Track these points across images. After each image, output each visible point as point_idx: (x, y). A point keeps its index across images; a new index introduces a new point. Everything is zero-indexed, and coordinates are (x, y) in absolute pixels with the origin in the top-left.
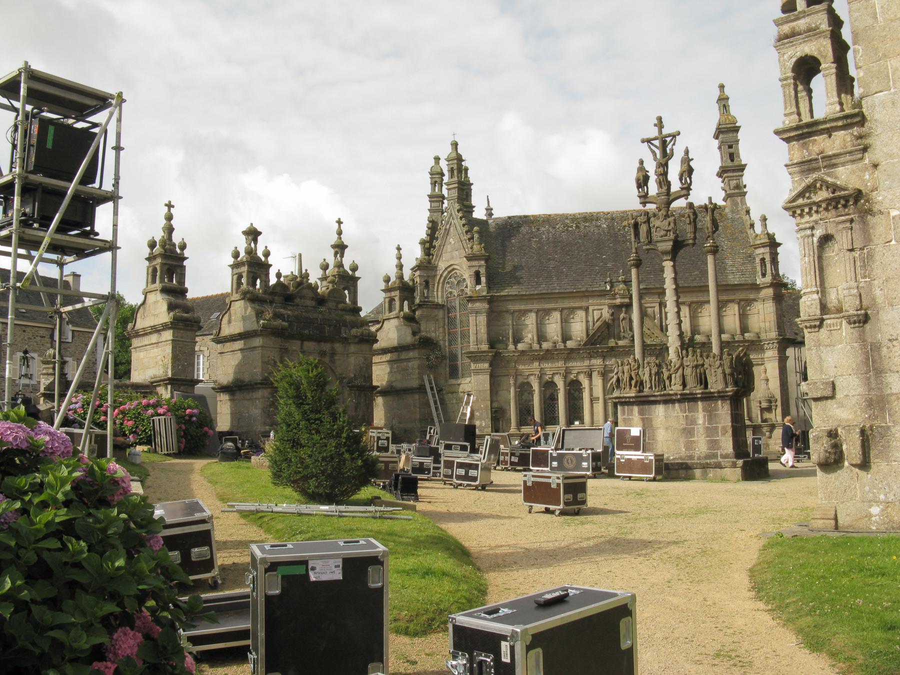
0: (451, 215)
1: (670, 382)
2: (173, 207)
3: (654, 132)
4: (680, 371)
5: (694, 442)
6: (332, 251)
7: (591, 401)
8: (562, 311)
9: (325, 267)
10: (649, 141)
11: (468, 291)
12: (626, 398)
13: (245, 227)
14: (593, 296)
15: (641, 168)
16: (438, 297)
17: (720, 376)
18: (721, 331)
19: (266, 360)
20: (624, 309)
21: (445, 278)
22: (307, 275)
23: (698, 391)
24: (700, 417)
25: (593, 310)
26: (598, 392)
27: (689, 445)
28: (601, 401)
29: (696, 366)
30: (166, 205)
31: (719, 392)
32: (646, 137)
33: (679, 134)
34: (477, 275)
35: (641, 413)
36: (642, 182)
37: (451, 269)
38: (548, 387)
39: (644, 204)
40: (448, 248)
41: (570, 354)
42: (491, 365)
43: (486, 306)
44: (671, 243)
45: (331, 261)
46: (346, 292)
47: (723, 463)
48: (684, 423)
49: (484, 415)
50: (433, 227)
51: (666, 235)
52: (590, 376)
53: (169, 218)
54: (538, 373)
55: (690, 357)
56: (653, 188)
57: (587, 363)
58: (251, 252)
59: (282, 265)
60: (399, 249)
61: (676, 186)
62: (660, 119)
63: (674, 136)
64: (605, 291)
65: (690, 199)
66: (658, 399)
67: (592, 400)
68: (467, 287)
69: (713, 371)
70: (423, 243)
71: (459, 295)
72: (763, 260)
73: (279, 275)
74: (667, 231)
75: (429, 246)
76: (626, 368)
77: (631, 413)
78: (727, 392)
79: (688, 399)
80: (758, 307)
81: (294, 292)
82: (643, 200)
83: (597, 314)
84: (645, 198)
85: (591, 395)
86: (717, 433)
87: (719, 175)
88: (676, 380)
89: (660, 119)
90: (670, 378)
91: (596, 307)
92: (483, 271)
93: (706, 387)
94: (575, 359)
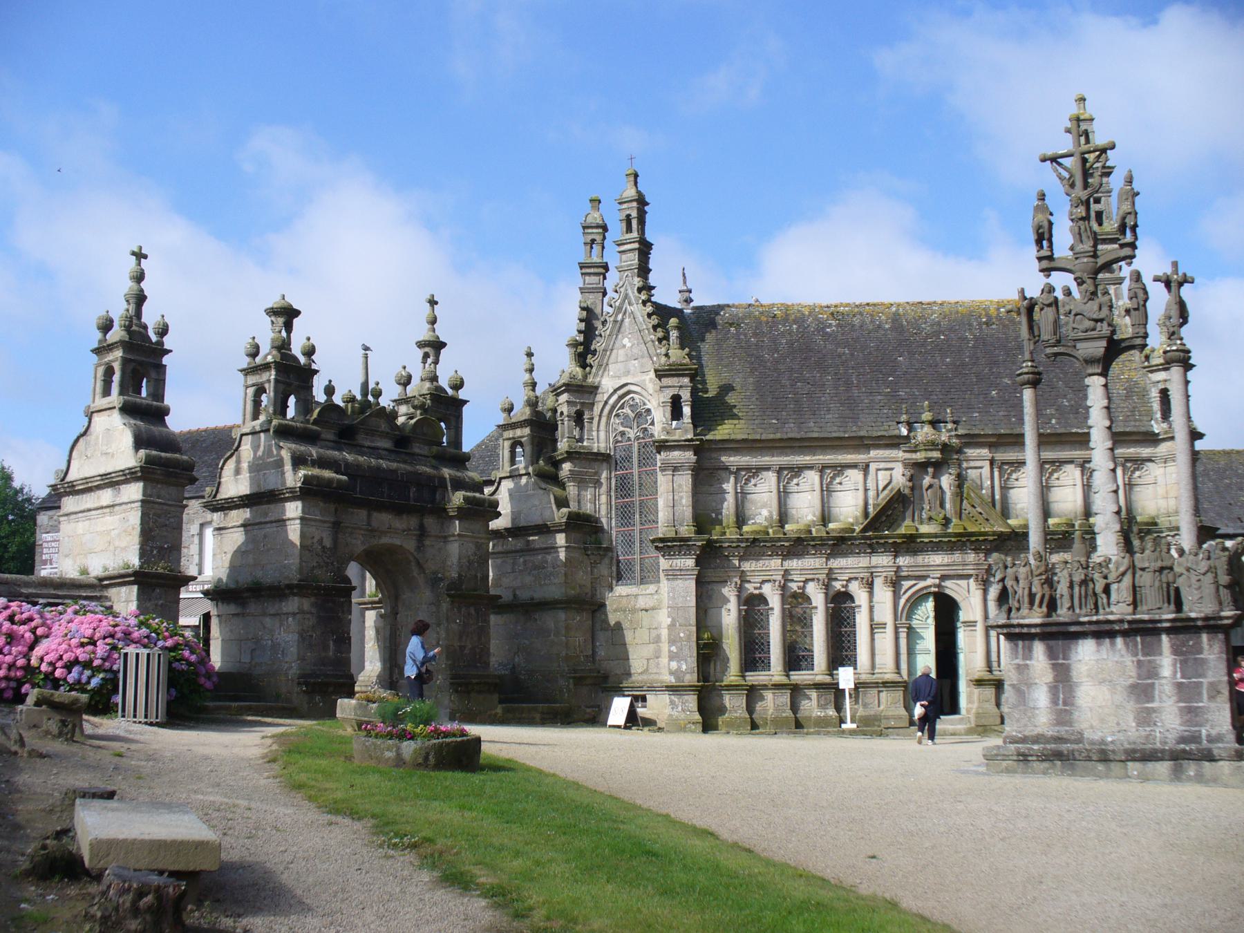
0: (626, 296)
1: (1109, 598)
2: (145, 257)
3: (1065, 143)
4: (1127, 580)
5: (1154, 710)
6: (420, 353)
7: (872, 629)
8: (822, 469)
9: (406, 381)
10: (1054, 159)
11: (658, 432)
12: (1022, 626)
13: (273, 301)
14: (878, 447)
16: (599, 439)
17: (1209, 589)
18: (1046, 513)
19: (309, 542)
20: (930, 470)
21: (613, 407)
22: (378, 394)
23: (1165, 617)
24: (1166, 663)
26: (885, 613)
27: (1146, 717)
28: (890, 629)
29: (1162, 569)
30: (134, 253)
31: (1206, 619)
32: (1050, 152)
34: (676, 403)
35: (1051, 654)
37: (623, 392)
38: (795, 603)
39: (1047, 271)
40: (618, 354)
41: (840, 544)
42: (698, 563)
43: (689, 456)
44: (1104, 343)
45: (417, 371)
46: (443, 424)
47: (1216, 752)
48: (1134, 674)
49: (686, 651)
50: (589, 319)
51: (1094, 329)
52: (870, 585)
53: (139, 277)
54: (779, 578)
55: (1147, 552)
58: (283, 346)
59: (338, 377)
64: (900, 437)
66: (1086, 628)
67: (874, 627)
68: (652, 423)
69: (1194, 579)
70: (574, 344)
71: (638, 438)
72: (1164, 394)
73: (330, 390)
74: (1096, 321)
75: (585, 349)
76: (1022, 571)
77: (1028, 654)
78: (1221, 618)
79: (1141, 631)
80: (1154, 471)
81: (353, 423)
82: (1045, 264)
83: (883, 478)
84: (1049, 264)
85: (872, 619)
86: (1200, 694)
88: (1121, 592)
90: (1107, 590)
91: (882, 465)
92: (686, 395)
93: (1179, 606)
94: (844, 554)
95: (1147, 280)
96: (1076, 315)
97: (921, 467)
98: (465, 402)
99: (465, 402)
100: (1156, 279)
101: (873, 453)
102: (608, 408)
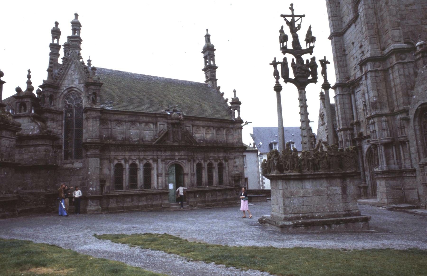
10: (284, 16)
20: (176, 126)
25: (160, 124)
32: (284, 14)
33: (304, 16)
36: (283, 38)
39: (284, 53)
51: (304, 73)
52: (157, 161)
56: (289, 45)
57: (155, 154)
60: (29, 71)
61: (304, 45)
62: (292, 5)
63: (301, 16)
65: (314, 55)
67: (158, 175)
68: (82, 102)
84: (285, 50)
87: (204, 70)
89: (292, 5)
91: (161, 123)
96: (298, 68)
97: (173, 124)
98: (4, 82)
99: (4, 82)
100: (320, 61)
101: (159, 119)
102: (62, 96)
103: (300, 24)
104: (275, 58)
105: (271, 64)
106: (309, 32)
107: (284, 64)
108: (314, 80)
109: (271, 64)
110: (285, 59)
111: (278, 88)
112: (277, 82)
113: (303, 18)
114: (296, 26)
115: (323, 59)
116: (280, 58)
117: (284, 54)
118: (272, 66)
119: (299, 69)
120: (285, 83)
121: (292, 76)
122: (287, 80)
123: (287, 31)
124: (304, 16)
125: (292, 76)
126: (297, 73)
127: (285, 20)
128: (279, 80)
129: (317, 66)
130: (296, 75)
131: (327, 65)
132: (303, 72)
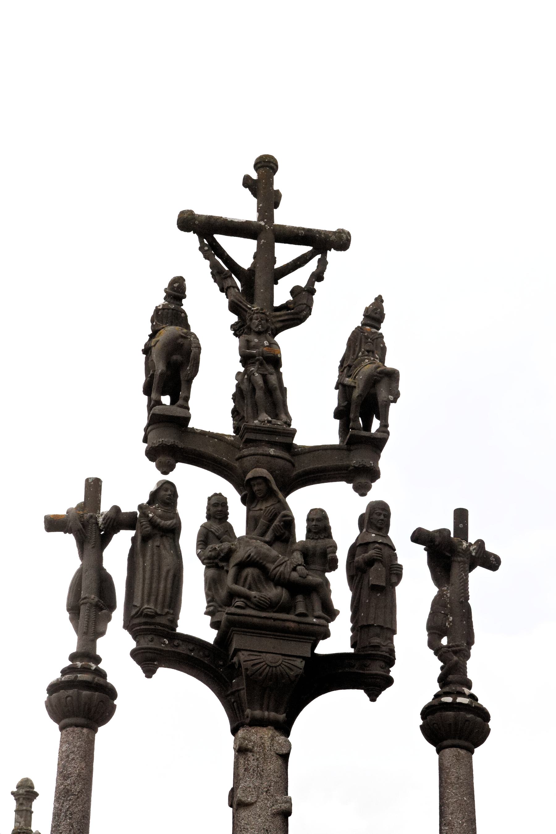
15: (171, 310)
32: (203, 209)
33: (341, 241)
51: (287, 608)
61: (314, 422)
62: (267, 165)
84: (171, 439)
89: (267, 165)
95: (399, 534)
96: (241, 566)
103: (310, 291)
104: (94, 487)
105: (53, 524)
106: (367, 340)
107: (156, 524)
108: (368, 669)
109: (53, 524)
110: (165, 496)
111: (82, 701)
112: (86, 656)
113: (332, 255)
114: (282, 294)
115: (448, 523)
116: (130, 485)
117: (166, 468)
118: (67, 542)
119: (249, 571)
120: (137, 669)
121: (195, 620)
122: (160, 647)
123: (211, 317)
124: (341, 241)
125: (195, 620)
126: (232, 595)
127: (211, 250)
128: (102, 646)
129: (395, 573)
130: (223, 617)
131: (478, 577)
132: (273, 592)
